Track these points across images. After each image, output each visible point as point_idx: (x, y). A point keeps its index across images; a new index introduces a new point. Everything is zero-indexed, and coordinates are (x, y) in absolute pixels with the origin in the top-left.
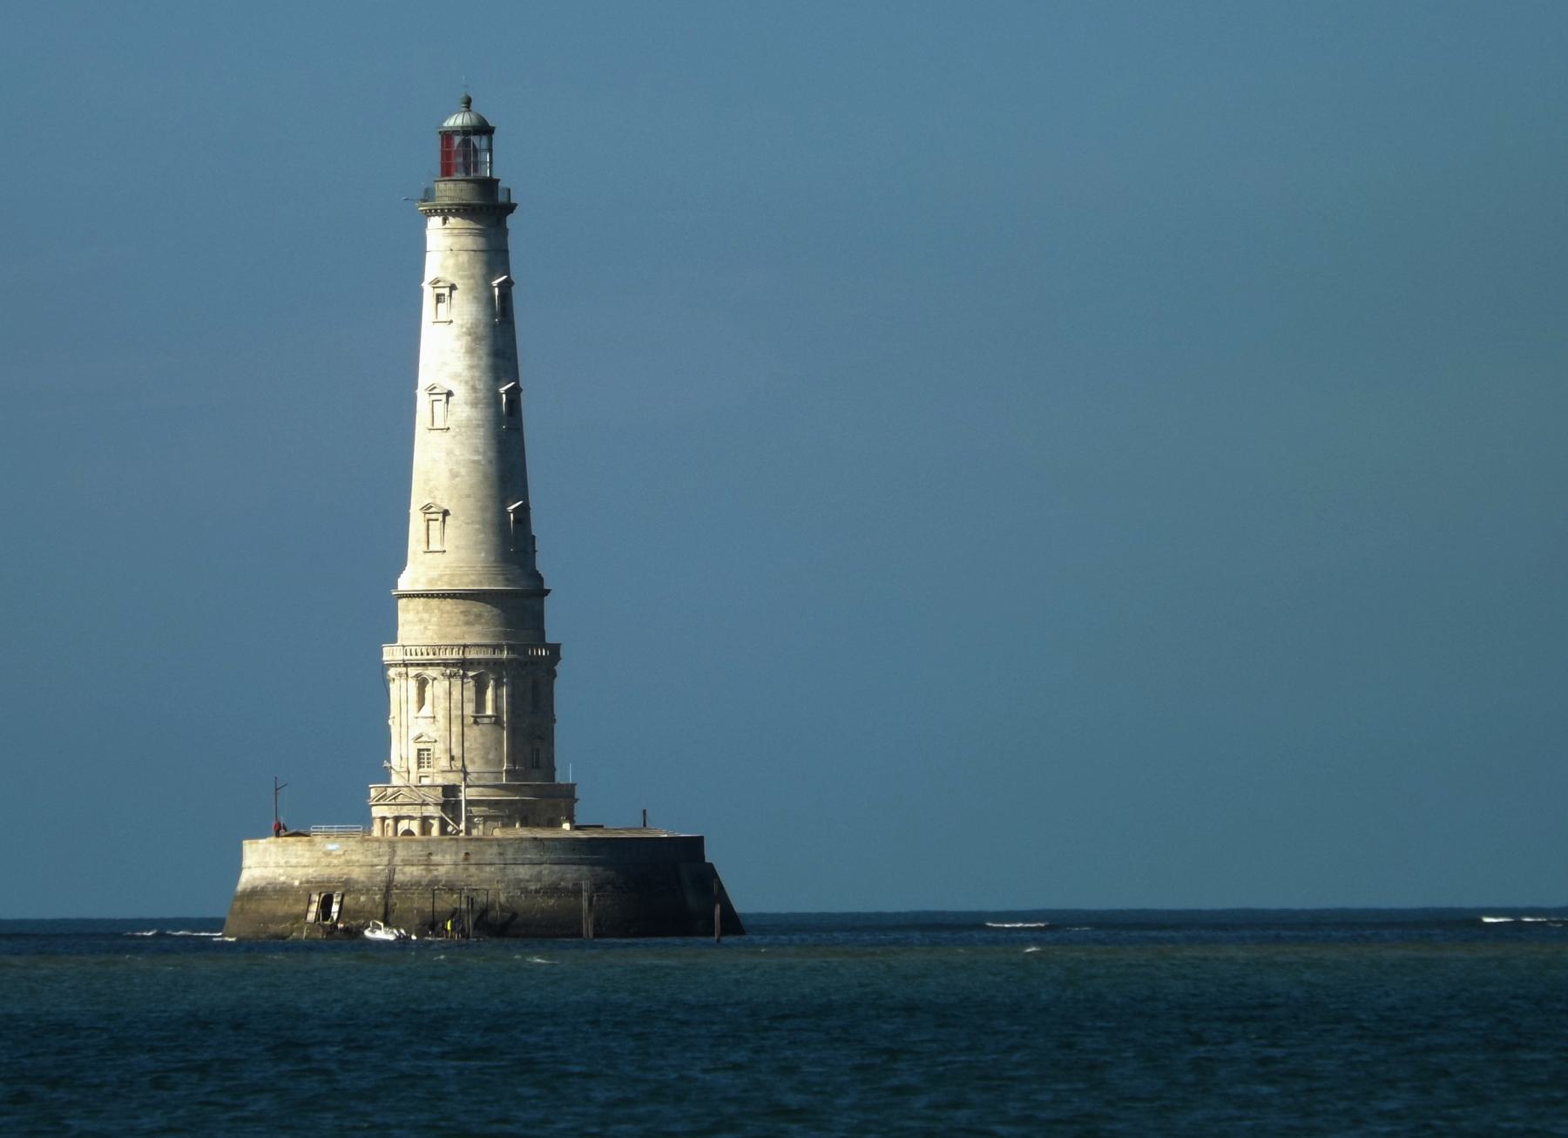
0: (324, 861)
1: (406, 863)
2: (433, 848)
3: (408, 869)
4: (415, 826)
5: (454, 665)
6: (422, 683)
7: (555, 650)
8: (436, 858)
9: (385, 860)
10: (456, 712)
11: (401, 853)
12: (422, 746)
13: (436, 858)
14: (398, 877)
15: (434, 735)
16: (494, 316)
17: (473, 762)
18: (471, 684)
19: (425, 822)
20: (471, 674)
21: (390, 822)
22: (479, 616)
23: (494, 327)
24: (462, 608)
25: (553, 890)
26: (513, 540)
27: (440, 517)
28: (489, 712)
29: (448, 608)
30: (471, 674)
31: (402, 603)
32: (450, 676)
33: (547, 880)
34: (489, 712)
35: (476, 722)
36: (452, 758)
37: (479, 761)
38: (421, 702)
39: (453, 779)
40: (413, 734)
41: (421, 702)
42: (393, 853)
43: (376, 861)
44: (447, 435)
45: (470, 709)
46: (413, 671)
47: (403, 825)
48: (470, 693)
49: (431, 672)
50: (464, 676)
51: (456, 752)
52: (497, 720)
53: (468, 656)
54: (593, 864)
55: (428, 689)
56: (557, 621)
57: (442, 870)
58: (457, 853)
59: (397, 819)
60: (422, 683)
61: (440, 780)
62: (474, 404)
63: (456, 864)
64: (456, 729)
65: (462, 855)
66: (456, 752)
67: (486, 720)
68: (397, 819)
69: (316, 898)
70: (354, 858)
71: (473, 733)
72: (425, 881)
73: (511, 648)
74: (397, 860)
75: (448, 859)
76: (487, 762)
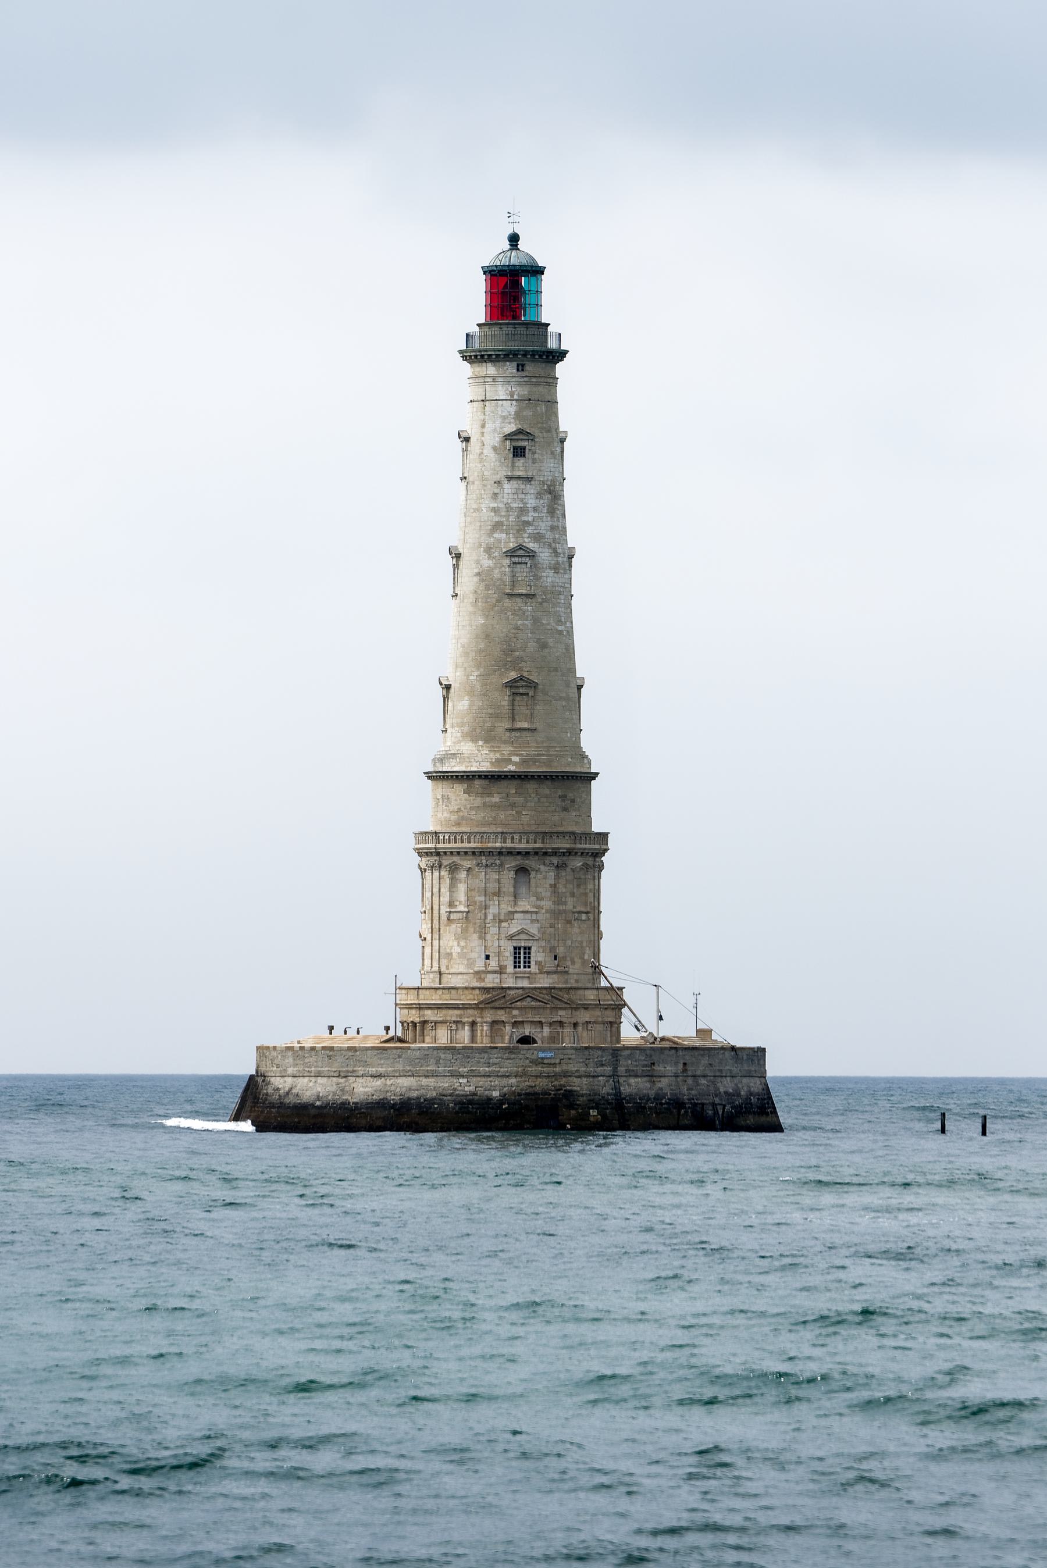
1: (631, 1073)
2: (655, 1058)
3: (632, 1081)
13: (659, 1068)
29: (547, 792)
58: (676, 1063)
65: (681, 1066)
72: (652, 1093)
75: (670, 1069)
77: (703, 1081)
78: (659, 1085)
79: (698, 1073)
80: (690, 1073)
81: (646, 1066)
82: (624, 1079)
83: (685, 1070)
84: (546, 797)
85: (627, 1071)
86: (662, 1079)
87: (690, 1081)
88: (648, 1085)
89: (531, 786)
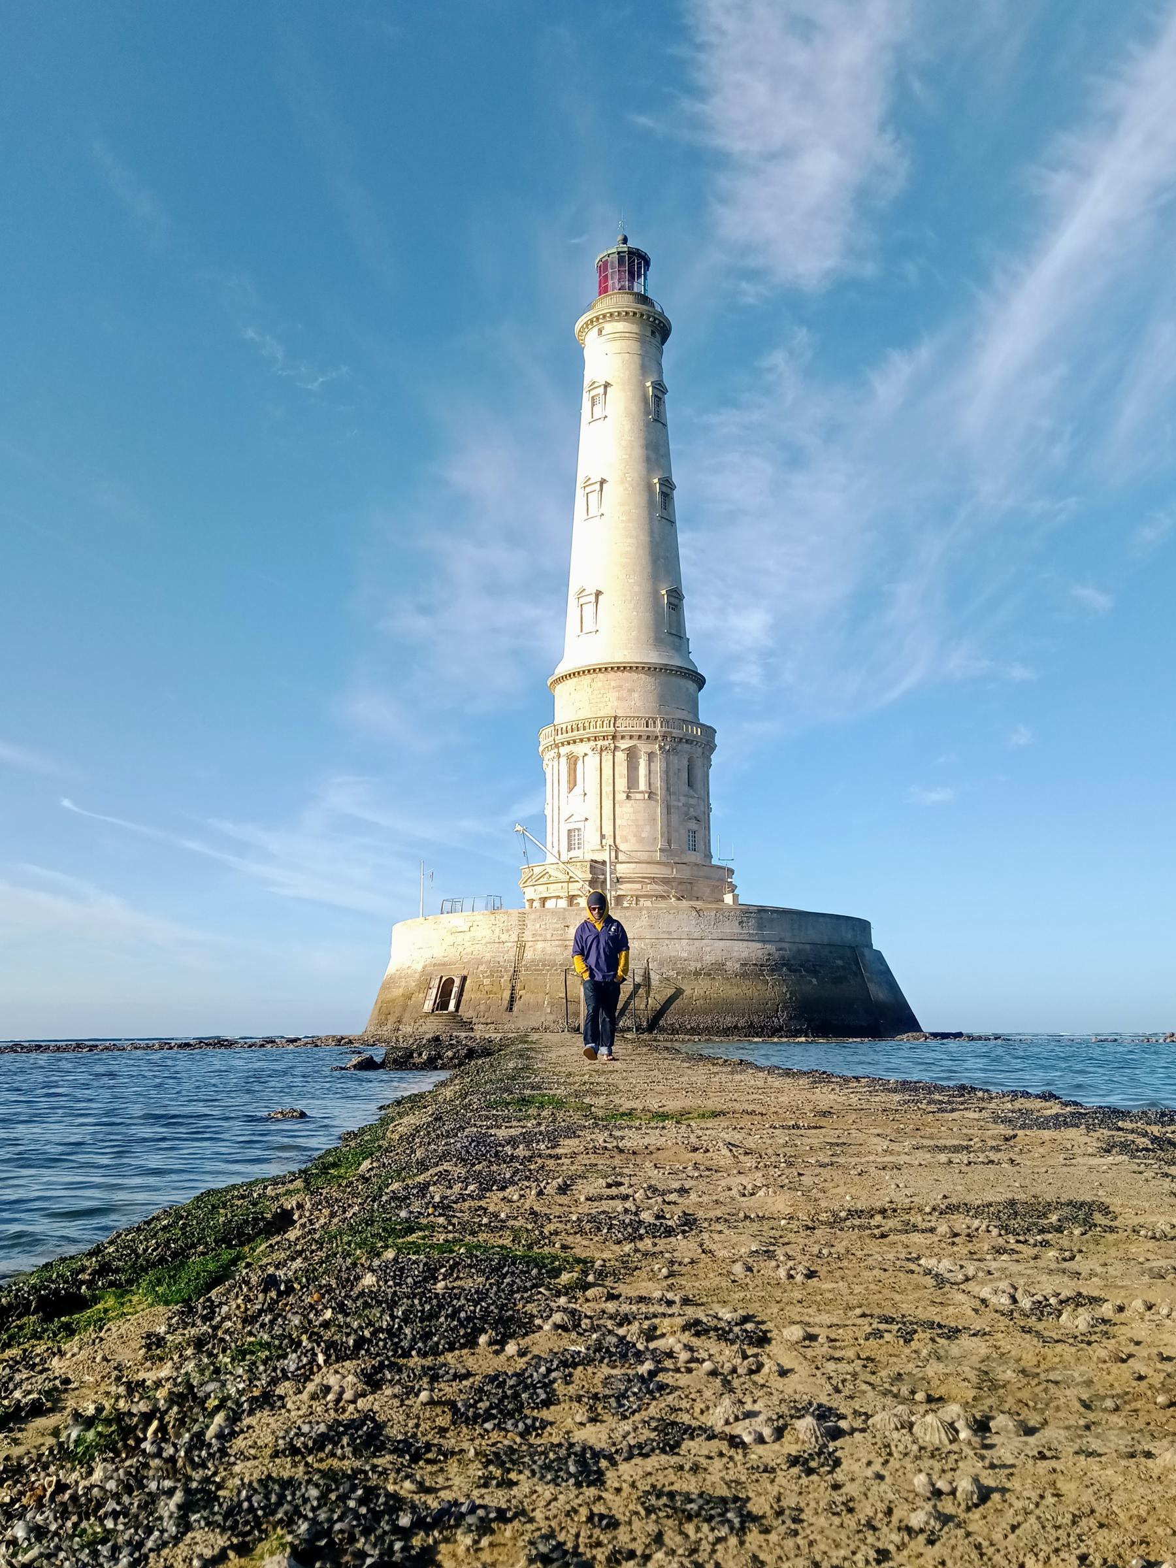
0: (450, 939)
3: (540, 945)
4: (563, 903)
6: (573, 761)
7: (710, 732)
10: (607, 789)
11: (532, 926)
12: (571, 826)
16: (647, 413)
17: (626, 840)
18: (621, 756)
19: (571, 899)
20: (624, 744)
21: (536, 904)
22: (631, 691)
23: (647, 425)
25: (716, 970)
26: (668, 616)
27: (593, 598)
28: (643, 785)
30: (624, 744)
31: (560, 691)
33: (709, 959)
34: (643, 785)
35: (628, 797)
36: (603, 837)
37: (633, 840)
38: (572, 784)
39: (603, 856)
40: (563, 817)
41: (572, 784)
42: (523, 925)
43: (504, 937)
45: (622, 783)
46: (564, 750)
47: (550, 904)
48: (622, 768)
49: (580, 749)
52: (651, 795)
54: (764, 942)
55: (580, 763)
56: (710, 708)
59: (544, 900)
60: (573, 761)
61: (590, 856)
66: (608, 830)
67: (639, 796)
68: (544, 900)
69: (435, 983)
71: (626, 811)
73: (665, 722)
74: (528, 936)
76: (641, 840)
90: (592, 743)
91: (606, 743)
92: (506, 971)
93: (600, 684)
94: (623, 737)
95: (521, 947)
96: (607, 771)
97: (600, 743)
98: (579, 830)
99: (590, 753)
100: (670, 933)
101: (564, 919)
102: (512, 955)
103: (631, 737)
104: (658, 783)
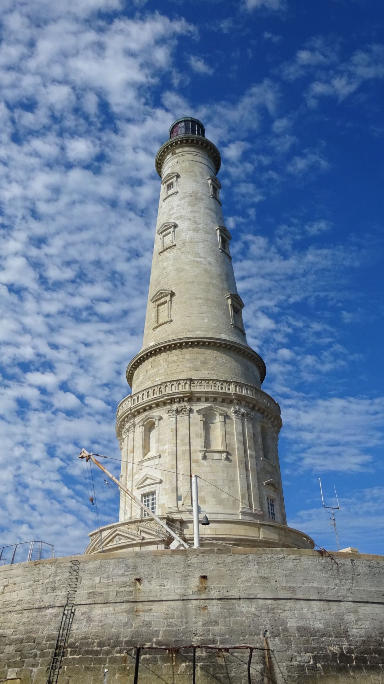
1: (97, 599)
2: (143, 571)
3: (98, 611)
5: (181, 400)
8: (149, 588)
9: (60, 597)
11: (87, 583)
12: (147, 490)
13: (149, 588)
14: (78, 629)
15: (157, 475)
18: (196, 418)
22: (204, 363)
24: (187, 356)
32: (178, 412)
35: (205, 458)
36: (179, 498)
41: (146, 448)
44: (175, 250)
45: (198, 444)
49: (157, 413)
50: (191, 411)
51: (183, 490)
53: (194, 389)
57: (159, 610)
62: (195, 230)
63: (185, 599)
64: (183, 466)
65: (195, 582)
67: (216, 456)
70: (15, 597)
71: (203, 468)
72: (126, 635)
74: (81, 596)
75: (172, 588)
77: (244, 607)
78: (146, 617)
79: (233, 593)
80: (214, 594)
81: (125, 584)
82: (83, 609)
83: (203, 589)
84: (174, 362)
85: (91, 594)
86: (155, 607)
87: (215, 608)
88: (124, 618)
89: (162, 357)
90: (168, 407)
91: (182, 404)
92: (43, 655)
93: (175, 358)
94: (199, 399)
95: (68, 610)
96: (183, 431)
97: (175, 406)
98: (153, 493)
99: (165, 416)
100: (292, 589)
101: (135, 567)
102: (52, 630)
103: (207, 400)
104: (236, 445)
